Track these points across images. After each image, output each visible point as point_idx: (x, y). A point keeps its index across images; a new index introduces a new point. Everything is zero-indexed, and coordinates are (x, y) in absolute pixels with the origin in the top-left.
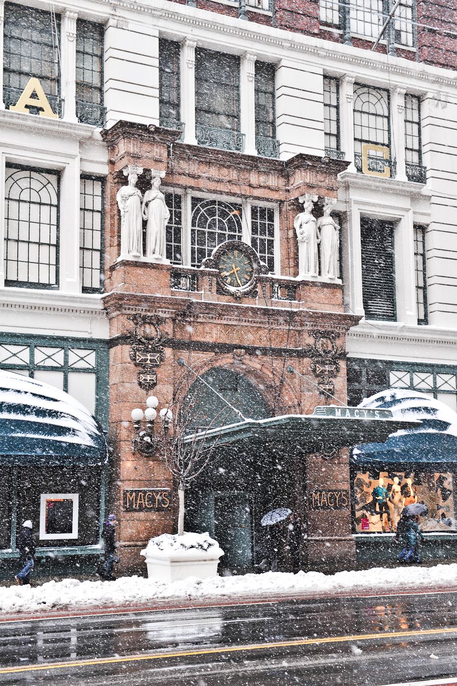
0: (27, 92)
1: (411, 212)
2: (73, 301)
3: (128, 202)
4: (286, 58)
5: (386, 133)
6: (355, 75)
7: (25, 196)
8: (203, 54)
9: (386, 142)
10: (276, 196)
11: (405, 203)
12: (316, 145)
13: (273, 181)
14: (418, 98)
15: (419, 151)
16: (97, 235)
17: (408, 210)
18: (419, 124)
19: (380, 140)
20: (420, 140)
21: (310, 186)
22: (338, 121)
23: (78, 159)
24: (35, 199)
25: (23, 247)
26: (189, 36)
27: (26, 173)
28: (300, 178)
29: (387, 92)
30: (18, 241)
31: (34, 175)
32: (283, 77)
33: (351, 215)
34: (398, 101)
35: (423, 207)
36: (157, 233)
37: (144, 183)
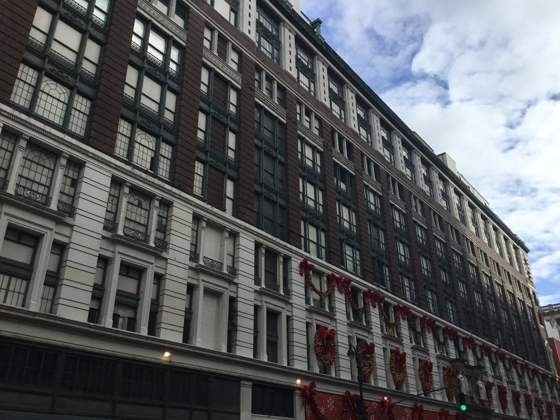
5: (146, 219)
18: (166, 218)
32: (88, 172)
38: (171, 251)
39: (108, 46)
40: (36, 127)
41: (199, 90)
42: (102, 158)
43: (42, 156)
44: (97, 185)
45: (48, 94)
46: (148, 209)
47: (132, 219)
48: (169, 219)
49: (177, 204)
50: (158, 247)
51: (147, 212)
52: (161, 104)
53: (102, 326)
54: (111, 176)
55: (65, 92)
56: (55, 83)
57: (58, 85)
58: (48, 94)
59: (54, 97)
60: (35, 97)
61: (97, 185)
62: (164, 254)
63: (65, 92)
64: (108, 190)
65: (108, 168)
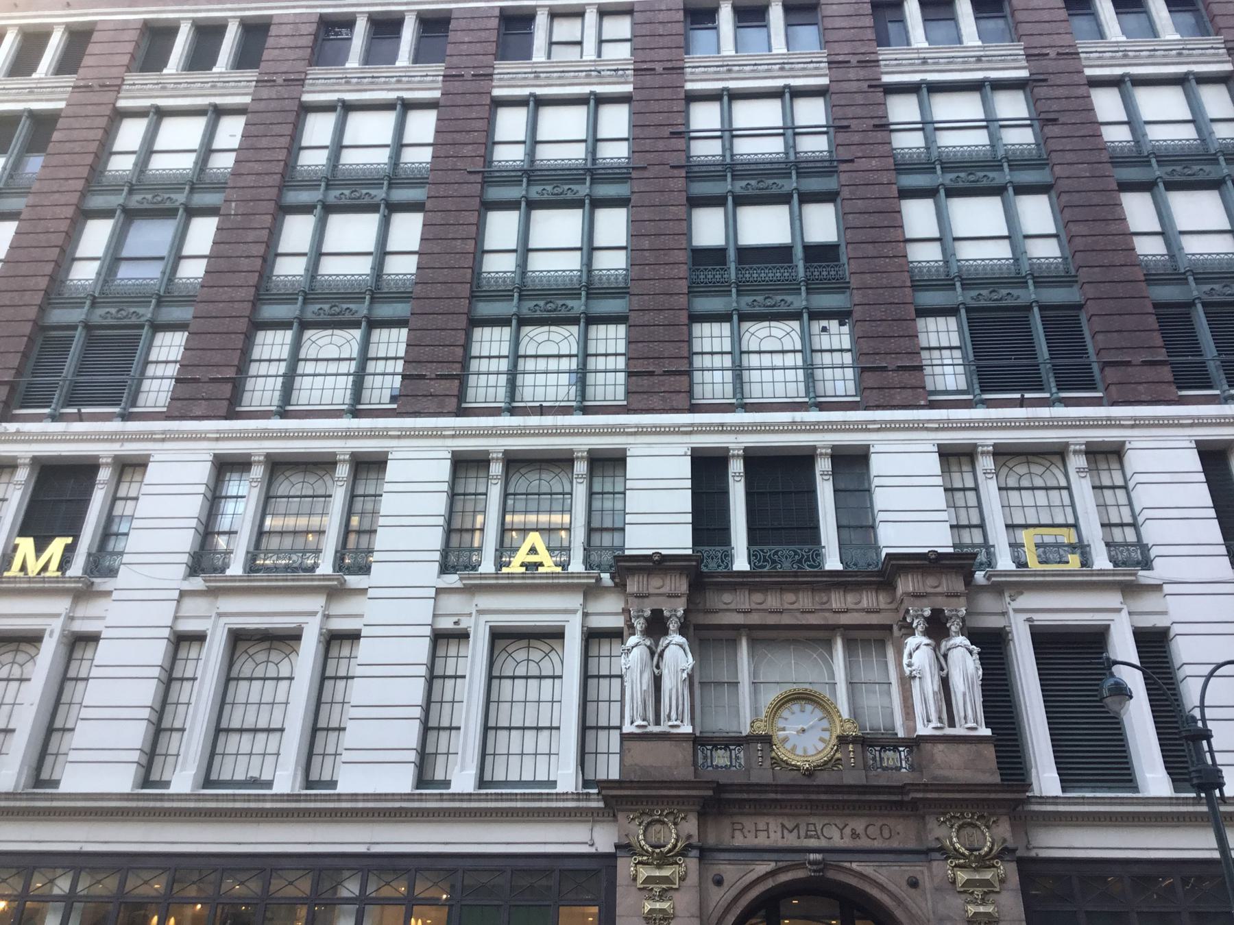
0: (525, 547)
1: (1124, 613)
2: (297, 801)
3: (631, 656)
4: (878, 442)
6: (992, 442)
7: (521, 671)
8: (756, 461)
9: (1071, 521)
10: (874, 619)
11: (1113, 599)
12: (939, 539)
13: (868, 599)
14: (1111, 454)
15: (1134, 525)
16: (616, 707)
17: (1119, 610)
18: (1125, 487)
19: (1060, 520)
20: (1132, 510)
21: (917, 596)
22: (1073, 505)
23: (579, 614)
24: (534, 670)
25: (530, 735)
26: (731, 446)
27: (524, 643)
28: (906, 585)
29: (1058, 453)
30: (524, 728)
31: (534, 643)
33: (1011, 632)
34: (1077, 462)
35: (1148, 602)
36: (671, 690)
37: (656, 627)
38: (1157, 563)
39: (845, 193)
40: (836, 422)
41: (1103, 147)
42: (471, 428)
43: (544, 476)
44: (908, 481)
45: (760, 352)
46: (1063, 483)
47: (1029, 522)
48: (1131, 484)
49: (1134, 439)
50: (1124, 564)
51: (1065, 493)
52: (1015, 236)
53: (1037, 794)
54: (449, 456)
55: (788, 329)
56: (766, 324)
57: (773, 324)
58: (760, 352)
59: (771, 352)
60: (738, 371)
61: (908, 481)
62: (1144, 576)
63: (788, 329)
64: (939, 481)
65: (924, 435)
